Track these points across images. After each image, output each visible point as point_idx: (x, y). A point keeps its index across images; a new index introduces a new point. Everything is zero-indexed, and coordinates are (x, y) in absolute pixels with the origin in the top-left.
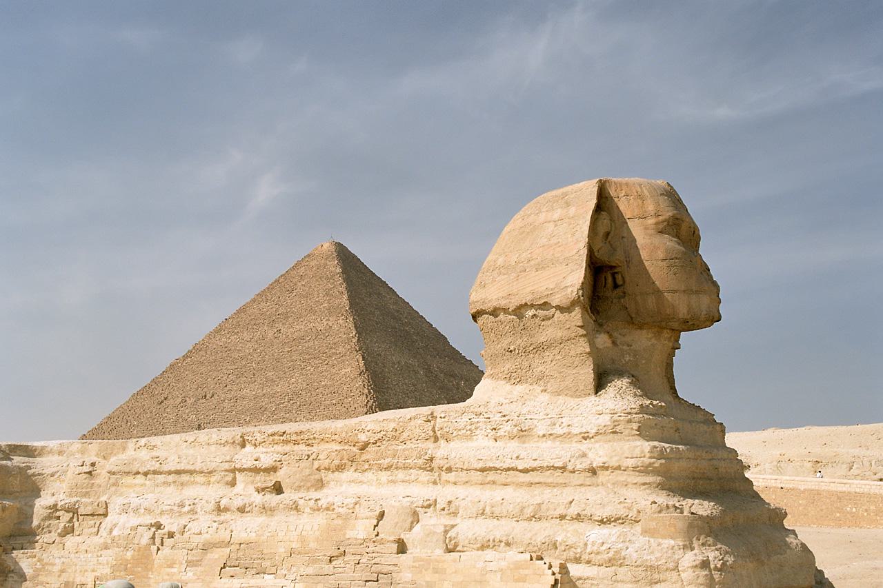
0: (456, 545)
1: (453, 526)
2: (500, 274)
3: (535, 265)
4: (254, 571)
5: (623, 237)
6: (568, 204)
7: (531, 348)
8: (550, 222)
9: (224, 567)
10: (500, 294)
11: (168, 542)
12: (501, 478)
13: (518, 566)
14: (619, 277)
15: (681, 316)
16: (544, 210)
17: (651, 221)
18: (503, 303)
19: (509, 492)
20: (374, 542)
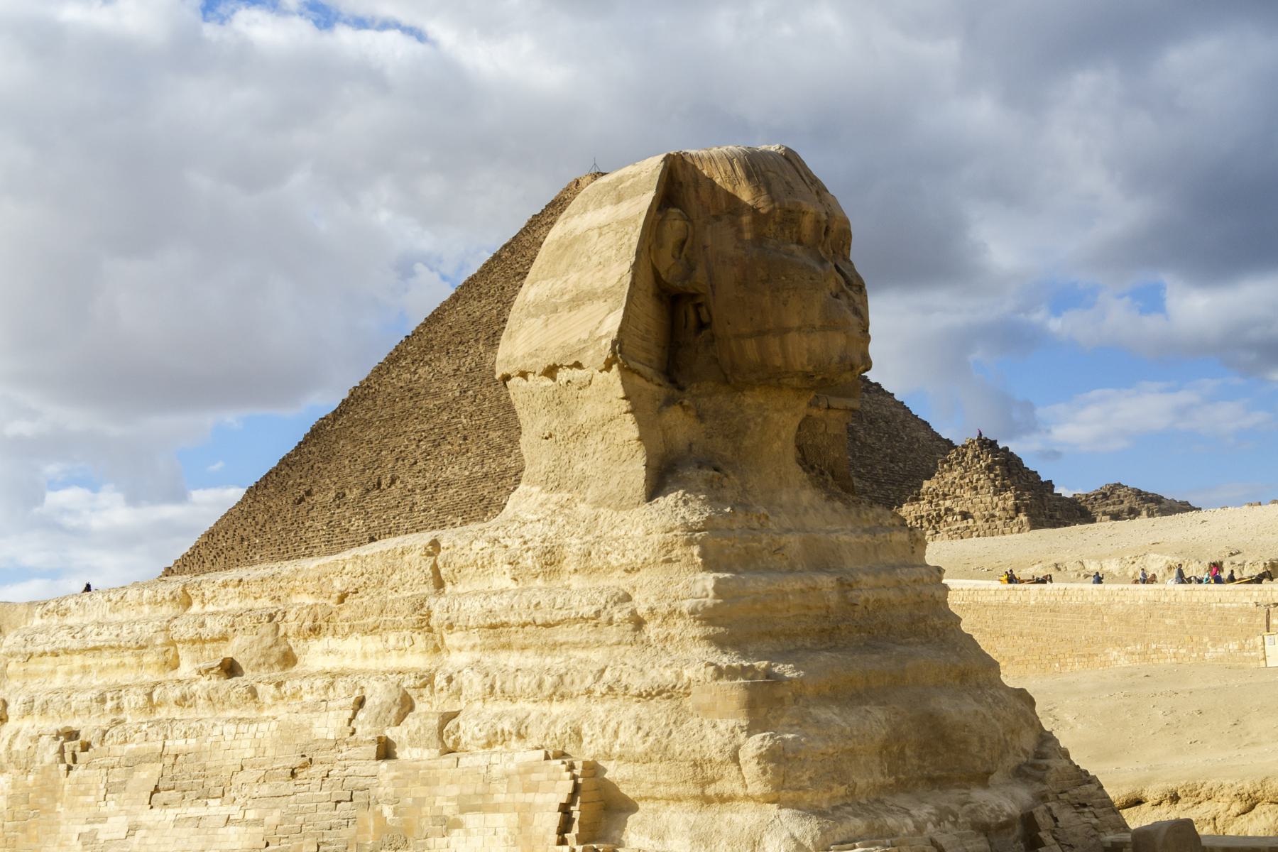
0: (457, 742)
1: (455, 715)
2: (529, 315)
3: (569, 301)
4: (193, 795)
5: (705, 247)
6: (619, 199)
7: (570, 433)
9: (157, 790)
11: (82, 757)
12: (518, 638)
13: (529, 769)
14: (703, 311)
15: (798, 367)
16: (591, 207)
18: (528, 364)
19: (530, 660)
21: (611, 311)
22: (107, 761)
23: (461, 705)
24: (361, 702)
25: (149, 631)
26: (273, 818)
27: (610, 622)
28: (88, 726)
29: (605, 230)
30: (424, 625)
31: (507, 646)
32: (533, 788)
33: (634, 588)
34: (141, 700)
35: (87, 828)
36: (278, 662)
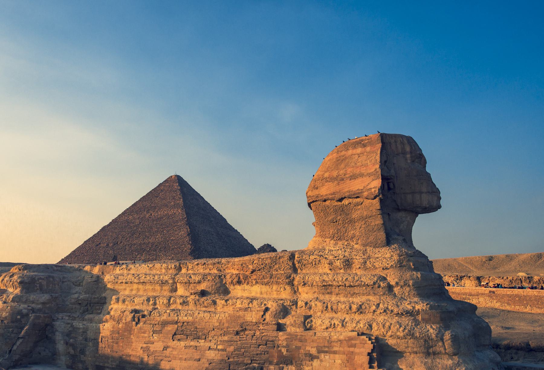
0: (311, 326)
2: (327, 181)
3: (349, 177)
5: (394, 164)
6: (364, 146)
8: (355, 155)
10: (329, 192)
13: (351, 339)
17: (408, 156)
20: (263, 324)
21: (373, 180)
22: (153, 322)
23: (311, 312)
24: (267, 309)
25: (166, 278)
26: (232, 349)
27: (379, 287)
28: (146, 308)
29: (361, 155)
30: (291, 283)
31: (331, 293)
32: (354, 346)
33: (387, 275)
34: (165, 301)
35: (145, 345)
36: (222, 293)
